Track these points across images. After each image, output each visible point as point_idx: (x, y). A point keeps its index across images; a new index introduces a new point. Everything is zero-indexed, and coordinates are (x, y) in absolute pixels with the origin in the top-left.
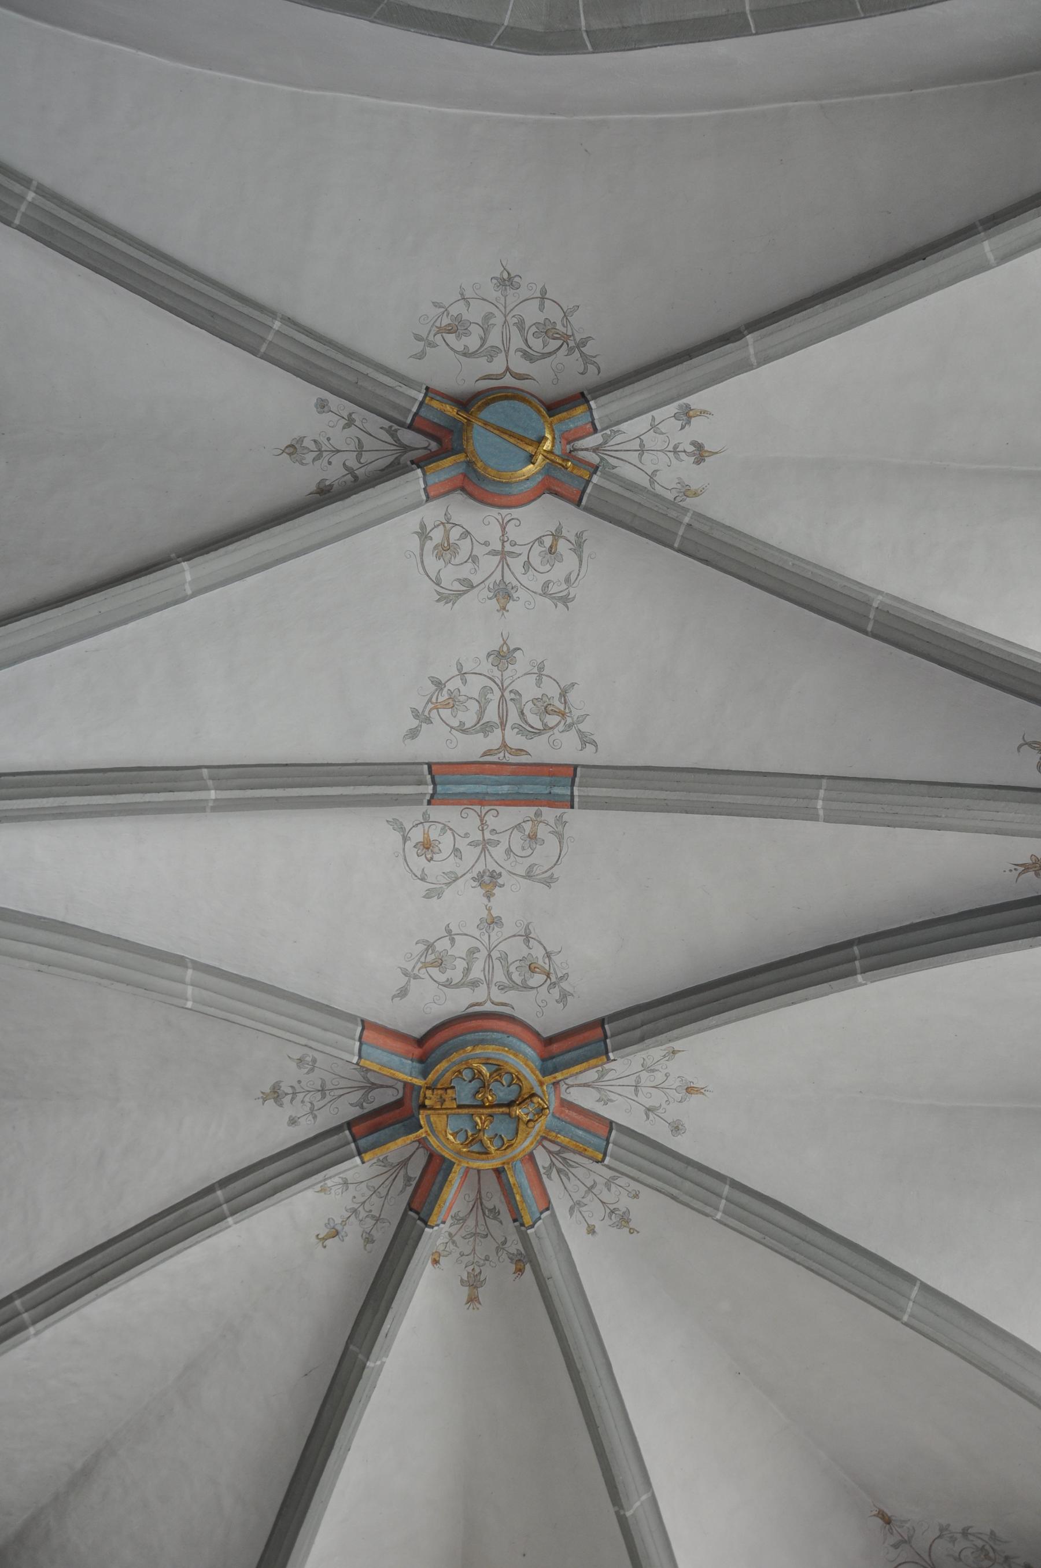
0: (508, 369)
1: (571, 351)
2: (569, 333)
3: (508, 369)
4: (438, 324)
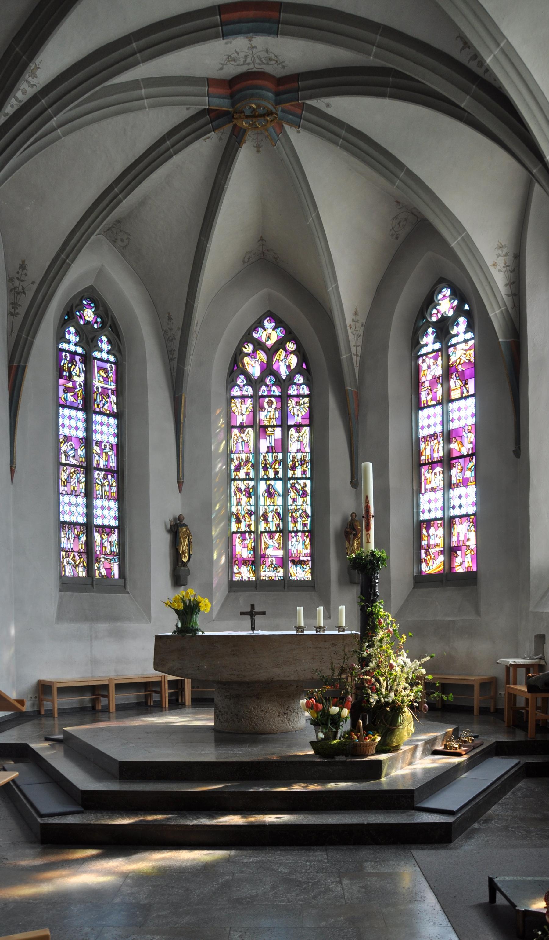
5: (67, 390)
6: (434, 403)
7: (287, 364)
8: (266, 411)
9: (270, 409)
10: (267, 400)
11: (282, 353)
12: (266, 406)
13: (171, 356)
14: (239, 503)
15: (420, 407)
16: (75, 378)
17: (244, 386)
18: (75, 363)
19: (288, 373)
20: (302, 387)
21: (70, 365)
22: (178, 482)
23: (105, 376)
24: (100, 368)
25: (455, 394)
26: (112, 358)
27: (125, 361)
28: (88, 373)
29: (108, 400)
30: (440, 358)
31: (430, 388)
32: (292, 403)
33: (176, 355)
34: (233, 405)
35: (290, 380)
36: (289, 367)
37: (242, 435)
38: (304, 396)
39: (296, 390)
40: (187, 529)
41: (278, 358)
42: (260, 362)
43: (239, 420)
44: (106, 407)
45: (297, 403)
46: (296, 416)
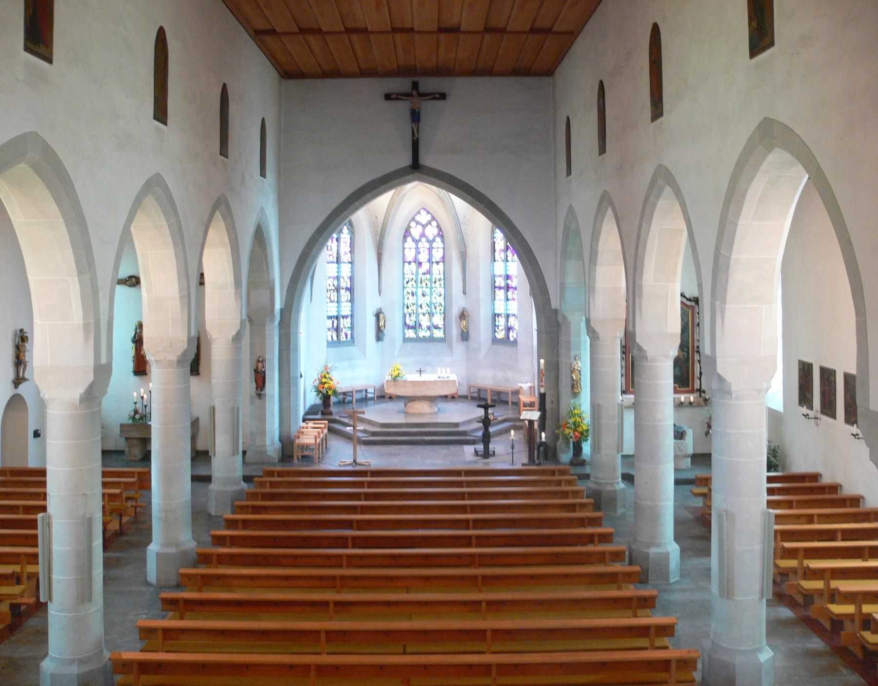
14: (408, 298)
22: (379, 291)
25: (509, 259)
35: (434, 240)
40: (384, 314)
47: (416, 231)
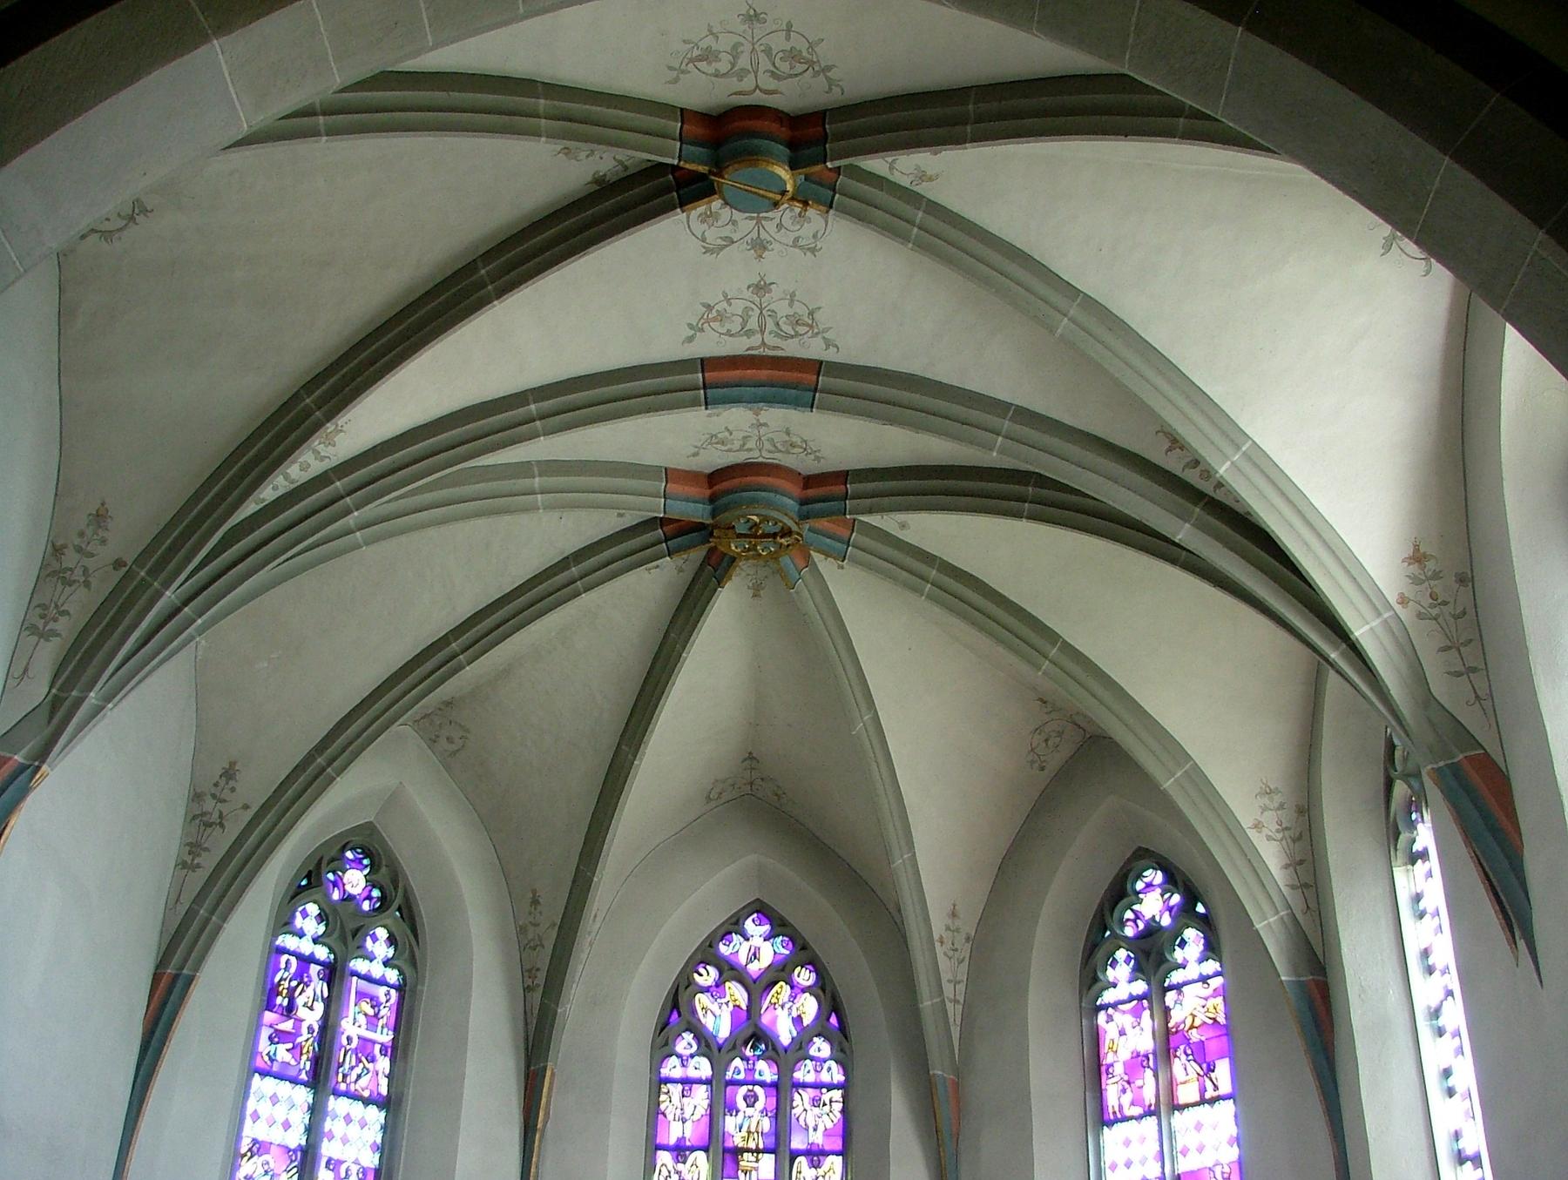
0: (757, 86)
1: (816, 74)
2: (815, 60)
3: (757, 86)
4: (689, 56)
5: (278, 1037)
6: (1137, 1111)
7: (795, 1014)
8: (741, 1115)
9: (750, 1111)
10: (743, 1090)
11: (782, 991)
12: (741, 1104)
13: (529, 982)
15: (1103, 1119)
16: (302, 1012)
17: (692, 1056)
18: (306, 980)
19: (795, 1034)
20: (826, 1066)
21: (294, 983)
23: (371, 1012)
24: (361, 995)
25: (1187, 1093)
26: (392, 976)
27: (423, 984)
28: (333, 1006)
29: (370, 1066)
30: (1146, 1014)
31: (1126, 1078)
32: (801, 1100)
33: (541, 978)
34: (663, 1097)
36: (798, 1020)
37: (680, 1167)
38: (830, 1087)
39: (812, 1072)
41: (774, 1000)
42: (731, 1005)
43: (674, 1132)
44: (364, 1082)
45: (816, 1102)
46: (811, 1130)
47: (717, 1017)
